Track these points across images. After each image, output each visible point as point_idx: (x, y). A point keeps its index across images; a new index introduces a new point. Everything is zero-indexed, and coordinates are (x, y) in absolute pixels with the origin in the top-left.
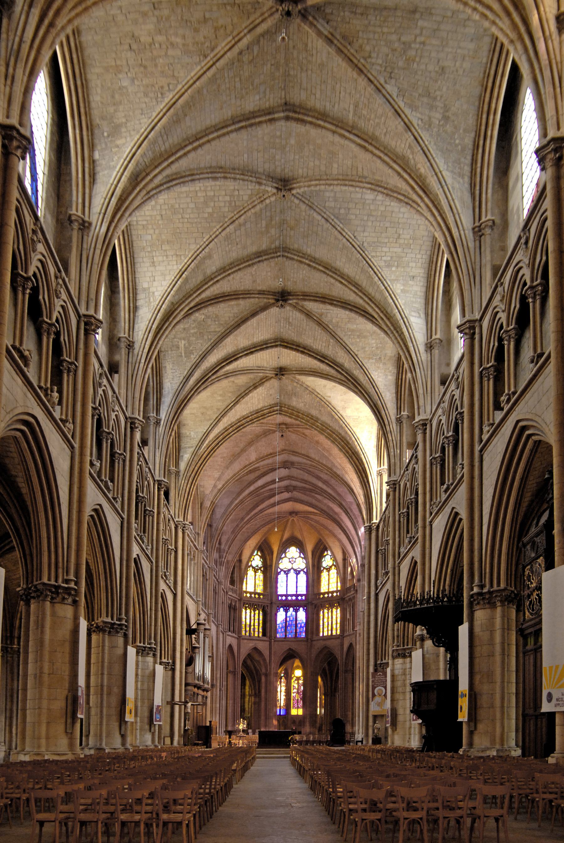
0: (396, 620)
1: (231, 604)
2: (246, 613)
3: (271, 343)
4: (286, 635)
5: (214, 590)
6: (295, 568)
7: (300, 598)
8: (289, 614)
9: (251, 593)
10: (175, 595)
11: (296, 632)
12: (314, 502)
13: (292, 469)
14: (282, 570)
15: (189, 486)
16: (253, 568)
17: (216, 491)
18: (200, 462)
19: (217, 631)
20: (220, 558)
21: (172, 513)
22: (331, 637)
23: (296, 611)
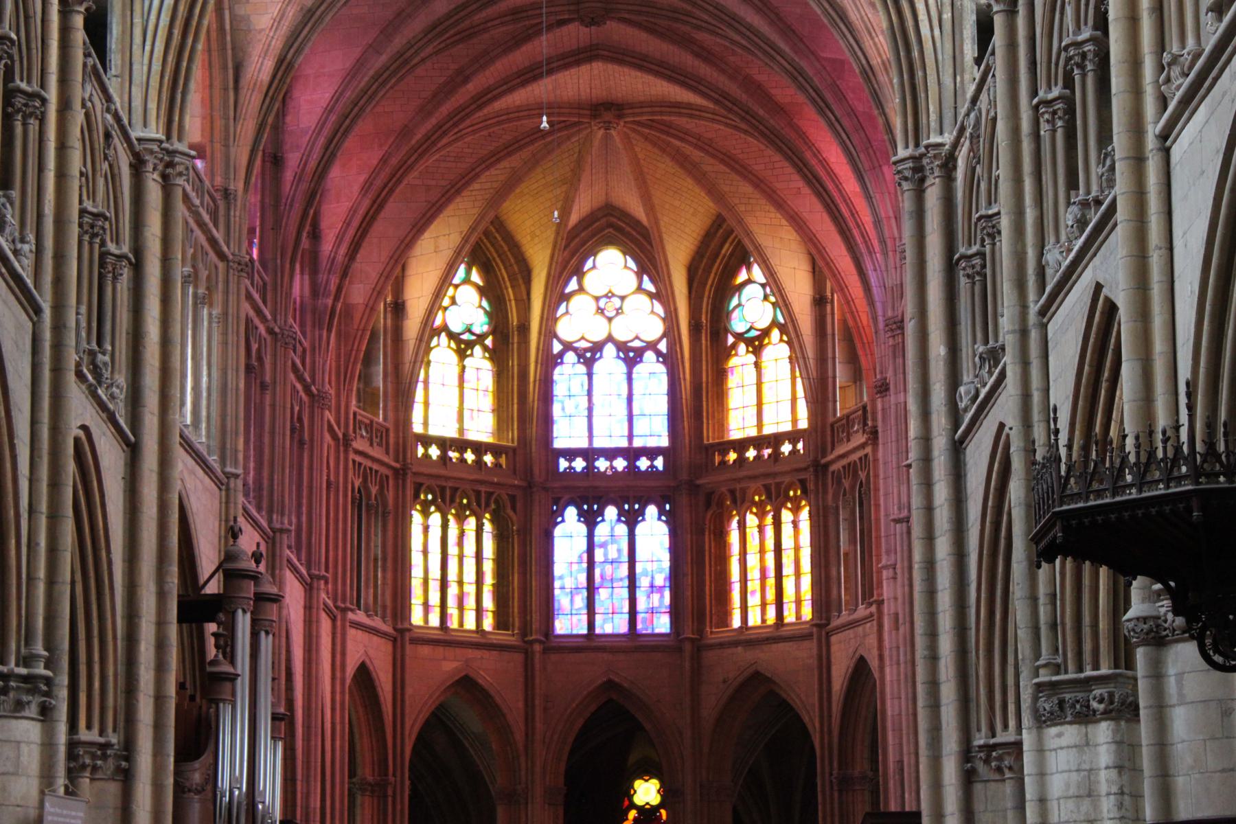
2: (426, 529)
4: (591, 624)
6: (621, 336)
7: (643, 464)
8: (602, 531)
9: (444, 444)
10: (133, 450)
11: (633, 612)
14: (568, 347)
16: (452, 336)
19: (308, 608)
22: (778, 634)
23: (632, 519)
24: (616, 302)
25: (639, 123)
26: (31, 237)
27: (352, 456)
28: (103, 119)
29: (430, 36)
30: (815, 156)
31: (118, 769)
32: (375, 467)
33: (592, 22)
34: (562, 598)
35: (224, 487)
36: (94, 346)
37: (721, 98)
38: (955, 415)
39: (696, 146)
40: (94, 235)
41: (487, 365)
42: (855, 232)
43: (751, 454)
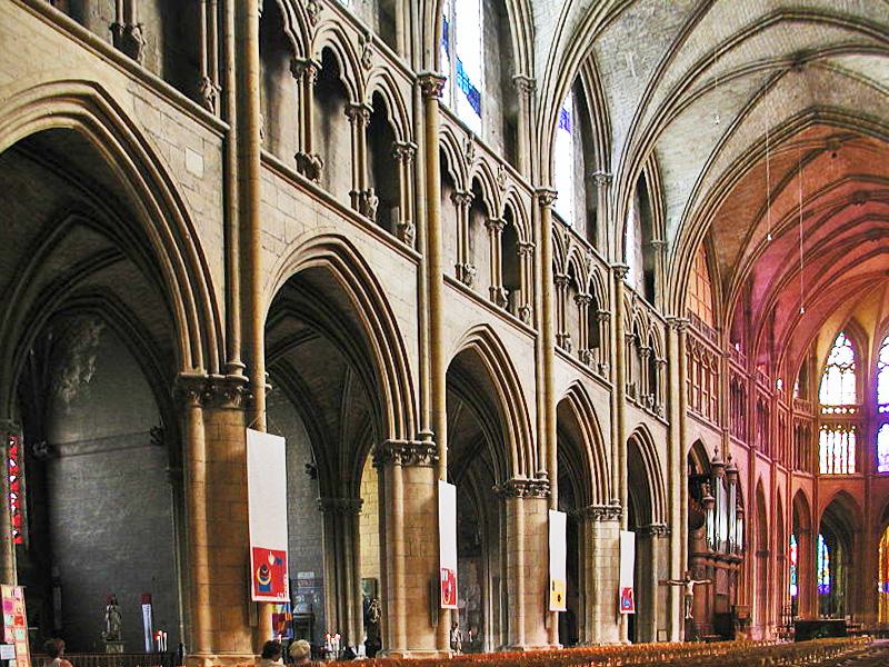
3: (768, 20)
18: (698, 224)
20: (772, 359)
26: (607, 362)
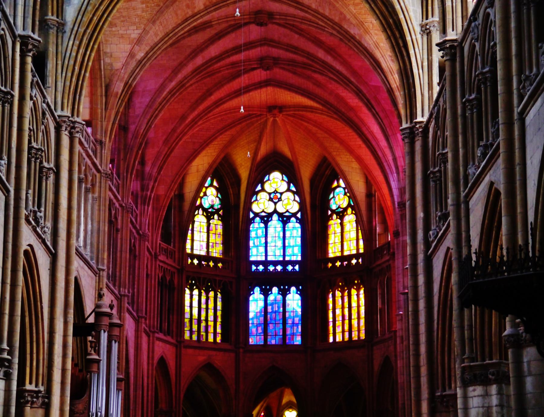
0: (464, 303)
1: (164, 277)
4: (265, 340)
5: (132, 251)
8: (271, 298)
9: (200, 258)
12: (310, 86)
13: (270, 26)
14: (256, 215)
15: (82, 51)
16: (205, 210)
17: (133, 64)
18: (102, 8)
19: (137, 331)
20: (142, 189)
21: (50, 99)
23: (284, 293)
24: (279, 195)
25: (289, 115)
27: (158, 262)
28: (42, 106)
29: (195, 74)
30: (367, 129)
31: (43, 403)
32: (169, 268)
33: (267, 68)
34: (253, 329)
35: (97, 275)
36: (36, 209)
37: (325, 103)
38: (427, 244)
39: (314, 126)
40: (36, 159)
41: (220, 223)
42: (385, 164)
43: (338, 264)
